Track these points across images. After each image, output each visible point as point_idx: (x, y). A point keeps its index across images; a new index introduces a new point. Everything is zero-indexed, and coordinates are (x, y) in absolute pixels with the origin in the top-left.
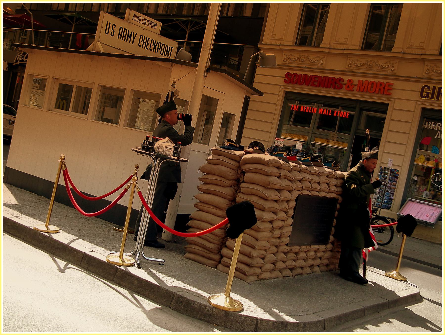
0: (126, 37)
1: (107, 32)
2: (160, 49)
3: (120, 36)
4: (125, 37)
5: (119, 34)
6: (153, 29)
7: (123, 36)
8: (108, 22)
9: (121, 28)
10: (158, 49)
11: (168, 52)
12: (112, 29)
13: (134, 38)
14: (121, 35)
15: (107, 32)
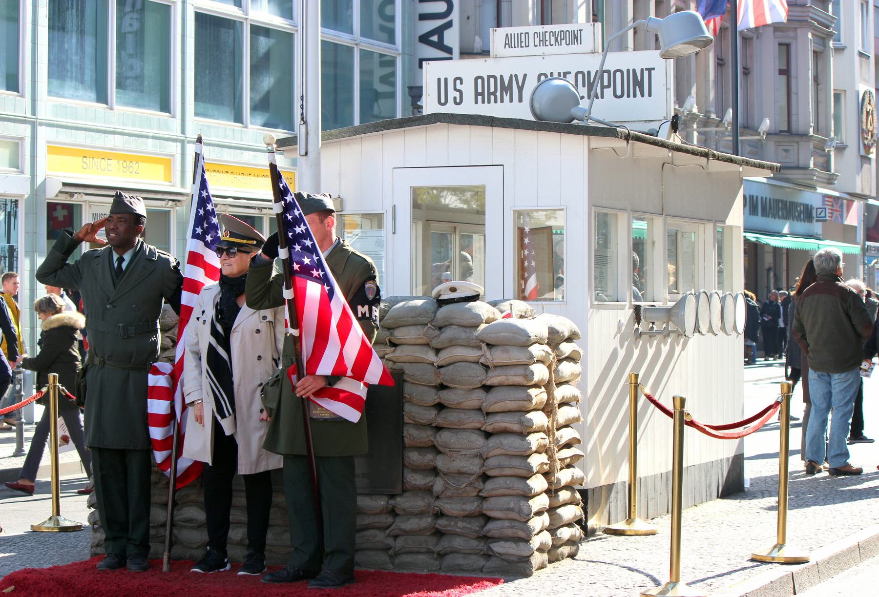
0: (498, 94)
1: (443, 101)
2: (608, 86)
3: (480, 98)
4: (494, 94)
5: (477, 94)
6: (573, 48)
7: (489, 94)
8: (439, 80)
9: (476, 79)
10: (603, 87)
11: (639, 84)
12: (455, 89)
13: (520, 89)
14: (482, 94)
15: (443, 101)
